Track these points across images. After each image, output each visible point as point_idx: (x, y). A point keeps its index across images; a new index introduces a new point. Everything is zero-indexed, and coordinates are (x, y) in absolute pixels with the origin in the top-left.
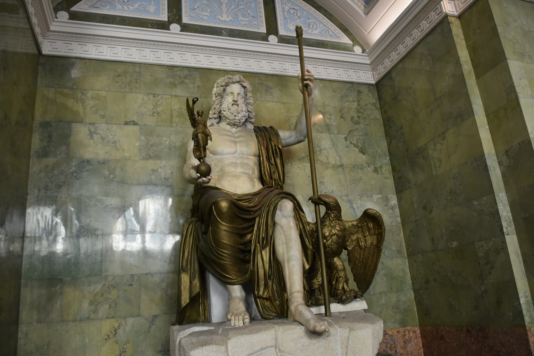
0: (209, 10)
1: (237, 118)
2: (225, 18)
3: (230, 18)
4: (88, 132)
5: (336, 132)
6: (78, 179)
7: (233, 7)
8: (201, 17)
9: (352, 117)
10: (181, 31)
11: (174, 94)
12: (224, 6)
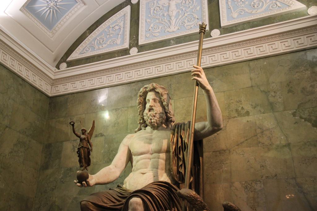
0: (160, 27)
1: (152, 121)
2: (172, 29)
3: (177, 28)
4: (72, 147)
5: (281, 109)
6: (63, 183)
7: (180, 16)
8: (154, 35)
9: (303, 88)
10: (138, 52)
11: (130, 105)
12: (173, 18)
